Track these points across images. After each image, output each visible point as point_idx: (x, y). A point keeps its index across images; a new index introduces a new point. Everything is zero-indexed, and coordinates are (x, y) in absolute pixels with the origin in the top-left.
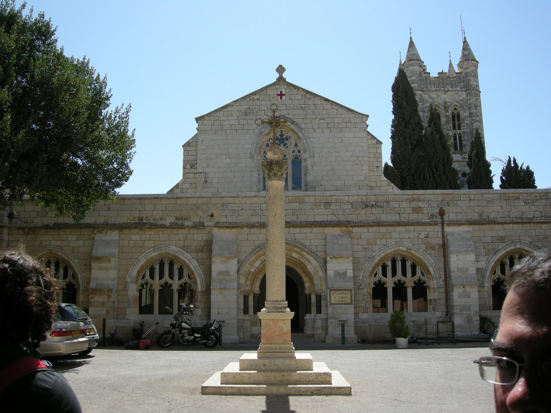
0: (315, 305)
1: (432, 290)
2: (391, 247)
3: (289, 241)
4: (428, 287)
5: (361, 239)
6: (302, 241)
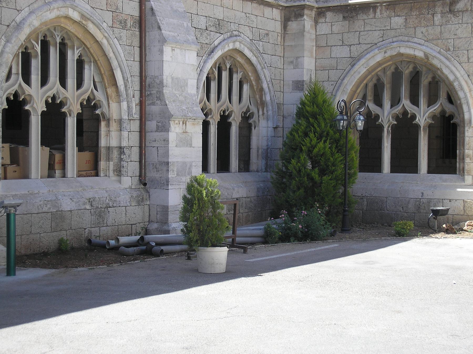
1: (114, 126)
4: (104, 117)
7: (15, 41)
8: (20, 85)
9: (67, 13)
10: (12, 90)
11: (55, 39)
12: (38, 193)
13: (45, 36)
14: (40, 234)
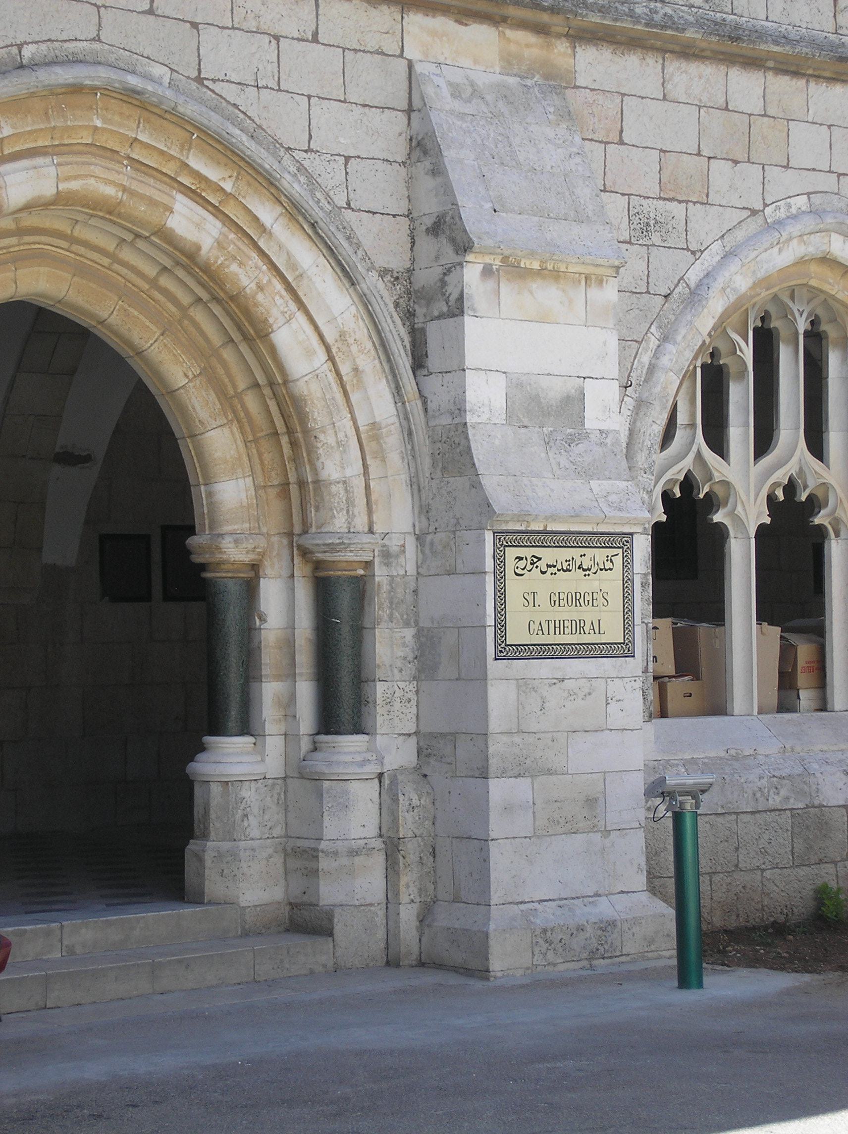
0: (305, 659)
2: (794, 229)
3: (158, 81)
5: (621, 142)
6: (247, 100)
7: (684, 337)
8: (699, 455)
9: (825, 248)
10: (677, 473)
11: (793, 323)
12: (754, 756)
13: (765, 318)
14: (763, 870)
